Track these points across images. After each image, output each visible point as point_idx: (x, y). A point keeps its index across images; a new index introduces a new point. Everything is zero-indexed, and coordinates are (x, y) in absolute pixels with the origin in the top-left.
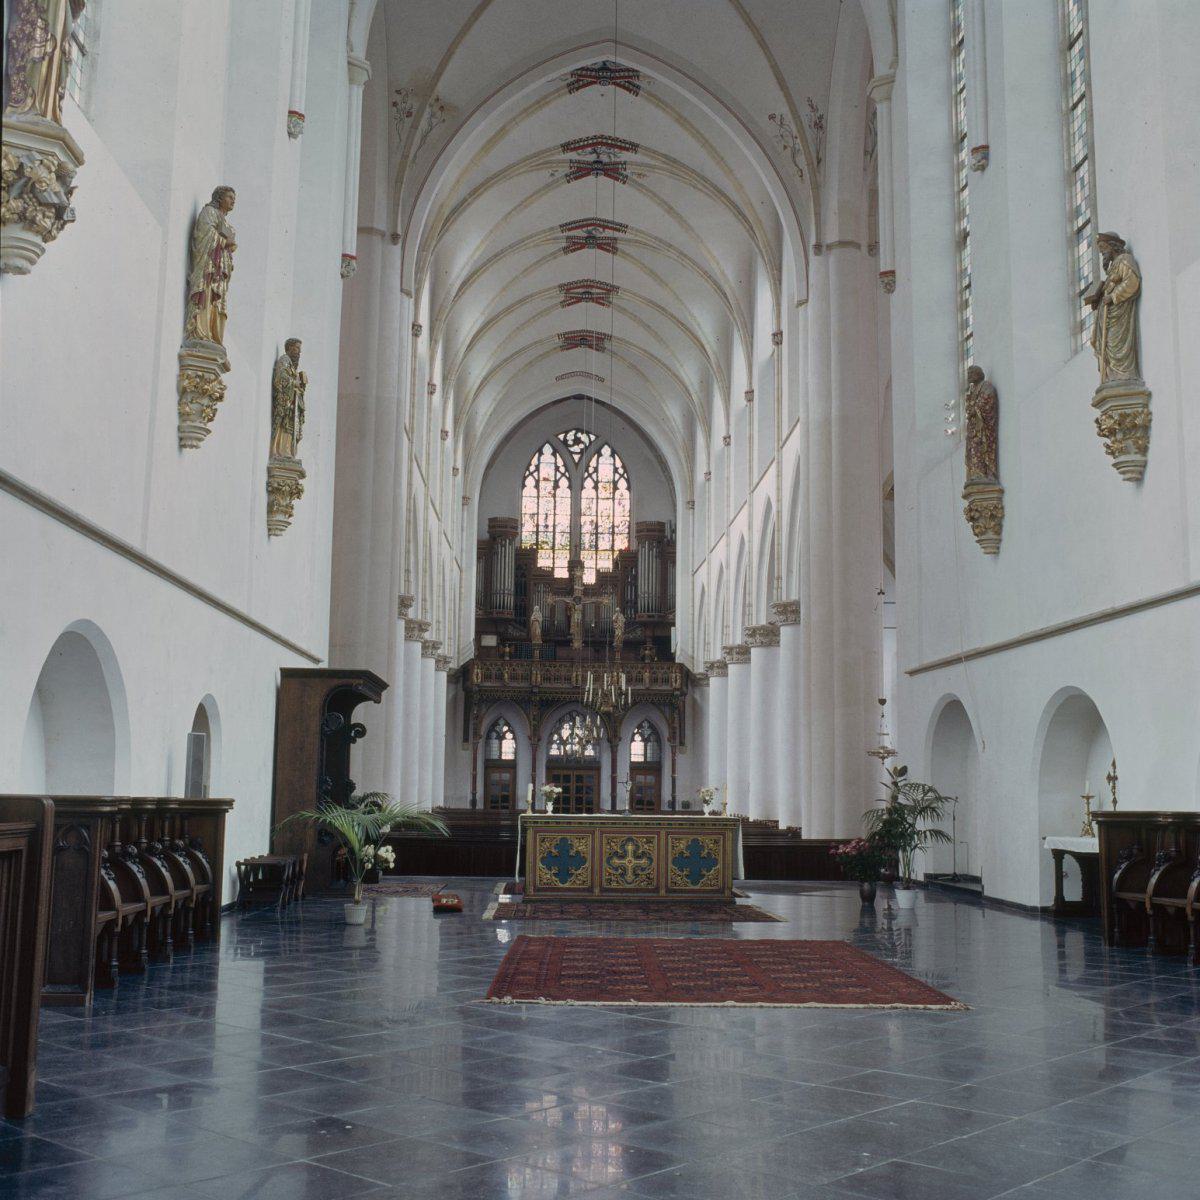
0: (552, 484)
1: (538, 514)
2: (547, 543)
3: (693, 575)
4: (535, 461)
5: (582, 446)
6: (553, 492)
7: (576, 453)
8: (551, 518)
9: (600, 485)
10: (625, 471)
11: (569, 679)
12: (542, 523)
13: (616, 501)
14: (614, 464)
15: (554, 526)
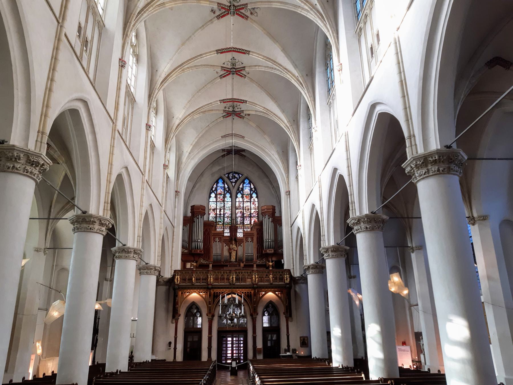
1: (216, 209)
2: (220, 222)
3: (291, 227)
4: (215, 186)
5: (236, 179)
6: (223, 199)
8: (222, 211)
11: (228, 279)
12: (218, 213)
13: (252, 203)
14: (250, 187)
15: (224, 214)
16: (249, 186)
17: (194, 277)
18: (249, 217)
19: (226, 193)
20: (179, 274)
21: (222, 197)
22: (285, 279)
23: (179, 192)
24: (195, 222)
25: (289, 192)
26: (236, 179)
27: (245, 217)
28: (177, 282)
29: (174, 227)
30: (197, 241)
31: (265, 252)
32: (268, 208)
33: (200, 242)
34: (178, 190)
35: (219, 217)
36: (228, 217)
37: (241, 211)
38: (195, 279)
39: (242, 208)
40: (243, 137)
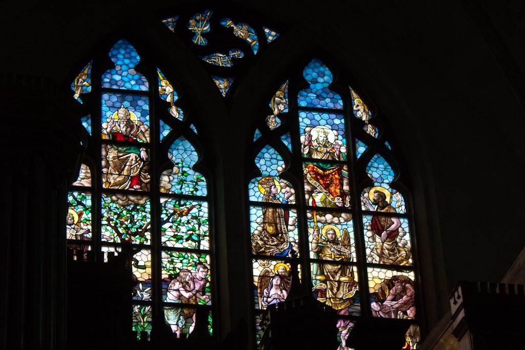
6: (146, 178)
7: (222, 73)
13: (367, 220)
16: (340, 104)
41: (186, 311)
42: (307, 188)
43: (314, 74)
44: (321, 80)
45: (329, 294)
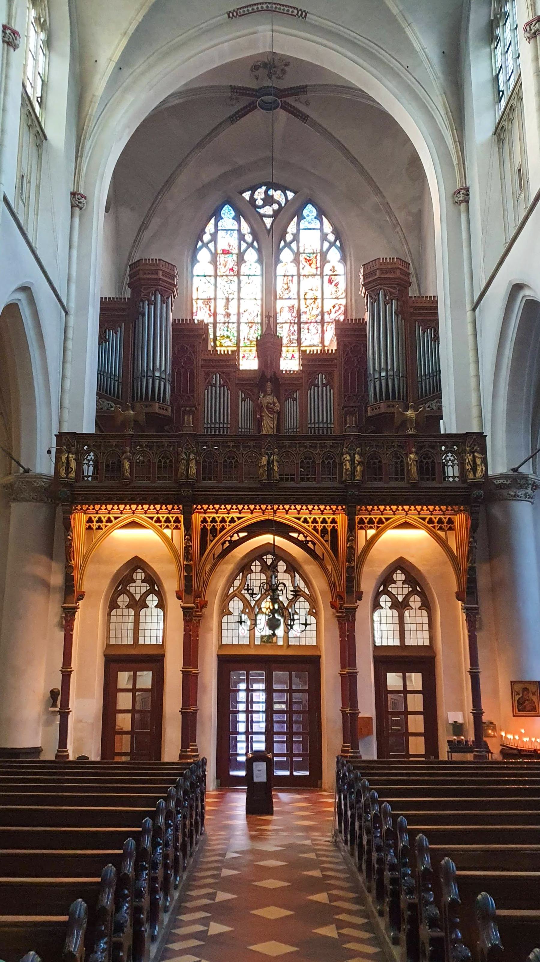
0: (235, 257)
1: (215, 299)
2: (228, 337)
3: (474, 310)
4: (210, 227)
6: (236, 268)
7: (269, 216)
9: (302, 258)
10: (338, 236)
12: (220, 310)
13: (326, 279)
17: (129, 460)
18: (316, 322)
19: (245, 251)
20: (74, 449)
21: (231, 261)
22: (468, 467)
23: (85, 198)
24: (144, 315)
25: (467, 189)
26: (276, 206)
27: (307, 323)
28: (67, 473)
29: (66, 313)
30: (150, 374)
31: (376, 412)
32: (383, 267)
33: (160, 378)
34: (81, 191)
35: (225, 323)
36: (251, 323)
37: (293, 306)
38: (131, 467)
39: (296, 297)
40: (302, 14)
41: (250, 325)
42: (301, 266)
43: (308, 213)
44: (310, 215)
45: (308, 313)
